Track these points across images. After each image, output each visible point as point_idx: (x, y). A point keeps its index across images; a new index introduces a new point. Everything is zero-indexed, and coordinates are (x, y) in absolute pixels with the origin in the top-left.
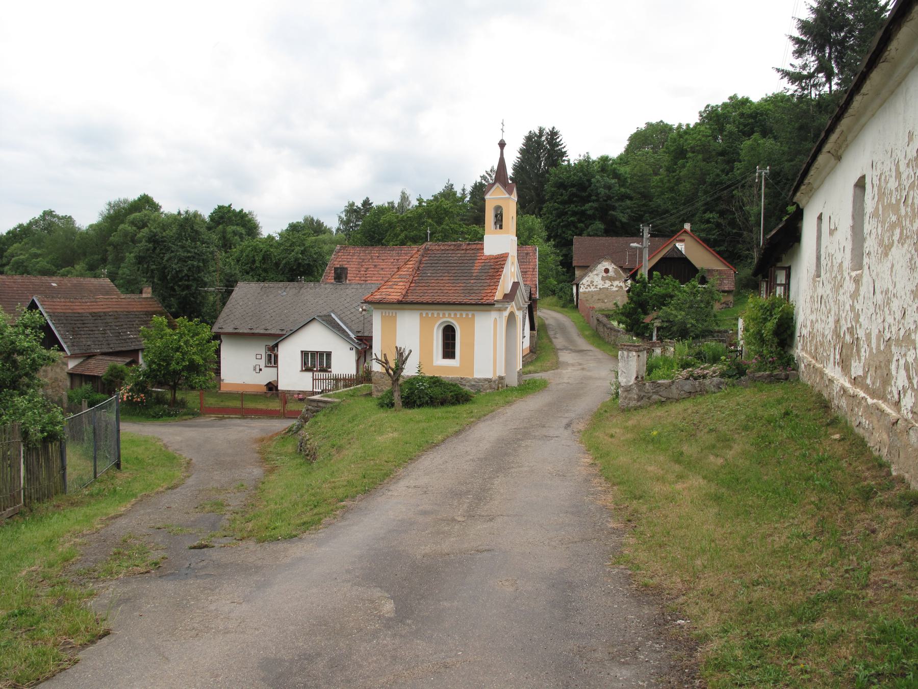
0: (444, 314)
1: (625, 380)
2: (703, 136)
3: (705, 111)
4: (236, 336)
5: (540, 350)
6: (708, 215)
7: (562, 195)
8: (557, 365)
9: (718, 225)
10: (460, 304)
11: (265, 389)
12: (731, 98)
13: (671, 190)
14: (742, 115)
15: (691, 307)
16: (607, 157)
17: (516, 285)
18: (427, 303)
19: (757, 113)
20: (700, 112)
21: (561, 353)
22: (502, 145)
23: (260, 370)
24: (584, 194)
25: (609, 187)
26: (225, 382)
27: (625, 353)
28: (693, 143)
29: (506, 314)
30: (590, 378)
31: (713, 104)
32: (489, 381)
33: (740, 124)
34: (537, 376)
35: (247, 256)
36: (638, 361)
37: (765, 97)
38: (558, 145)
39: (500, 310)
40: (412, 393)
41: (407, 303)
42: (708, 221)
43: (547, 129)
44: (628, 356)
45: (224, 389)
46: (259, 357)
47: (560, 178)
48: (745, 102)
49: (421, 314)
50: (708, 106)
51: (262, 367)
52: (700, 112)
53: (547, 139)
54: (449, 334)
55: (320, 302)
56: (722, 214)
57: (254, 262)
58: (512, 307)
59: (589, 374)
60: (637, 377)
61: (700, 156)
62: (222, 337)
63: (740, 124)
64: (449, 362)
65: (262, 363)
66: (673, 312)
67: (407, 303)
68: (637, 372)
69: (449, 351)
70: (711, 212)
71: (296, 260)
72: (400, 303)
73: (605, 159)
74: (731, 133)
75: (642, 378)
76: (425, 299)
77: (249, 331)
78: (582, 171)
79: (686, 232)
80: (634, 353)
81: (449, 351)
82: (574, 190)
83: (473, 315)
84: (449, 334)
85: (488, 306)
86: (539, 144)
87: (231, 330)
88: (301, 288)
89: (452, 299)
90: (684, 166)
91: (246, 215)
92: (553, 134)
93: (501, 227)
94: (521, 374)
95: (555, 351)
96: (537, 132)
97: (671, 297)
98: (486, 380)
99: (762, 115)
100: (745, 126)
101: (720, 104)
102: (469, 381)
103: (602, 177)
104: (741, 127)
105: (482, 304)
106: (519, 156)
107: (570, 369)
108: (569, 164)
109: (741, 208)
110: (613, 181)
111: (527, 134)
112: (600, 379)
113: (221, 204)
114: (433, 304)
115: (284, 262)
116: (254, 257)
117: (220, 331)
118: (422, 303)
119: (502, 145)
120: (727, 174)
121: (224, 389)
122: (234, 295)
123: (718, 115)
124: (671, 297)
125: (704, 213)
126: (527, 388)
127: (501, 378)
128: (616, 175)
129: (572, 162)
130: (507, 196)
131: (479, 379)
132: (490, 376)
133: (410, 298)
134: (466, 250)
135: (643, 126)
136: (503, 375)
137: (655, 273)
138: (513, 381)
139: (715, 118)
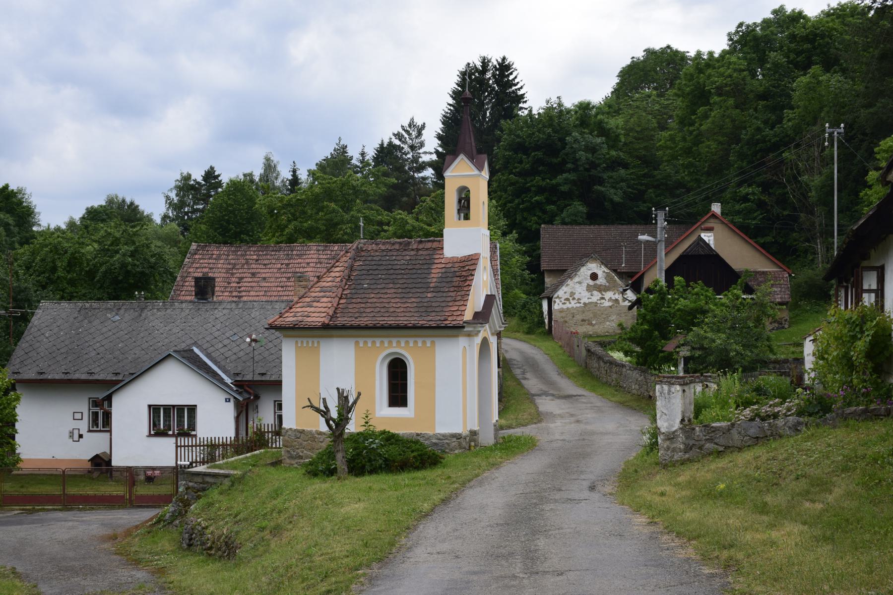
0: (390, 343)
1: (666, 424)
2: (735, 70)
3: (737, 32)
4: (44, 385)
5: (511, 393)
6: (744, 190)
7: (521, 162)
8: (538, 417)
9: (761, 204)
10: (415, 327)
11: (89, 466)
12: (775, 12)
13: (688, 152)
14: (793, 37)
15: (733, 328)
16: (589, 104)
17: (490, 299)
18: (367, 328)
19: (816, 35)
20: (729, 34)
21: (539, 401)
23: (81, 436)
24: (555, 161)
25: (592, 149)
27: (666, 387)
28: (720, 81)
29: (478, 340)
30: (593, 433)
31: (749, 21)
32: (457, 436)
33: (790, 51)
34: (517, 432)
35: (43, 260)
36: (684, 397)
37: (826, 8)
38: (511, 84)
39: (469, 335)
40: (359, 454)
41: (336, 328)
42: (745, 199)
43: (495, 59)
44: (669, 391)
46: (78, 416)
47: (518, 136)
48: (798, 16)
49: (357, 343)
50: (741, 25)
51: (84, 431)
52: (729, 34)
53: (494, 75)
54: (397, 372)
55: (175, 330)
56: (766, 187)
57: (54, 269)
58: (485, 331)
59: (589, 427)
60: (683, 420)
61: (731, 101)
63: (790, 51)
65: (83, 426)
66: (709, 335)
67: (336, 328)
68: (683, 412)
69: (398, 397)
70: (749, 186)
71: (124, 265)
72: (325, 327)
73: (584, 107)
74: (776, 65)
75: (689, 420)
76: (364, 321)
77: (63, 377)
78: (551, 125)
79: (714, 216)
80: (678, 387)
81: (398, 397)
82: (539, 154)
83: (433, 343)
84: (397, 372)
85: (455, 329)
86: (482, 83)
87: (32, 375)
88: (142, 310)
89: (402, 321)
90: (706, 116)
91: (13, 194)
92: (504, 68)
93: (467, 217)
94: (499, 428)
95: (530, 397)
96: (479, 65)
97: (704, 312)
98: (454, 436)
99: (823, 36)
100: (798, 53)
101: (759, 21)
103: (582, 133)
104: (792, 56)
105: (446, 327)
106: (451, 101)
107: (559, 423)
108: (530, 114)
109: (795, 178)
110: (599, 140)
111: (462, 67)
112: (607, 434)
114: (375, 327)
115: (103, 269)
116: (53, 261)
118: (359, 328)
120: (772, 128)
122: (35, 320)
123: (756, 39)
124: (704, 312)
125: (740, 185)
126: (509, 447)
127: (473, 433)
128: (602, 130)
129: (535, 112)
130: (476, 172)
131: (444, 436)
132: (458, 429)
133: (341, 320)
134: (418, 250)
135: (640, 54)
136: (476, 428)
137: (676, 278)
138: (488, 438)
139: (748, 41)
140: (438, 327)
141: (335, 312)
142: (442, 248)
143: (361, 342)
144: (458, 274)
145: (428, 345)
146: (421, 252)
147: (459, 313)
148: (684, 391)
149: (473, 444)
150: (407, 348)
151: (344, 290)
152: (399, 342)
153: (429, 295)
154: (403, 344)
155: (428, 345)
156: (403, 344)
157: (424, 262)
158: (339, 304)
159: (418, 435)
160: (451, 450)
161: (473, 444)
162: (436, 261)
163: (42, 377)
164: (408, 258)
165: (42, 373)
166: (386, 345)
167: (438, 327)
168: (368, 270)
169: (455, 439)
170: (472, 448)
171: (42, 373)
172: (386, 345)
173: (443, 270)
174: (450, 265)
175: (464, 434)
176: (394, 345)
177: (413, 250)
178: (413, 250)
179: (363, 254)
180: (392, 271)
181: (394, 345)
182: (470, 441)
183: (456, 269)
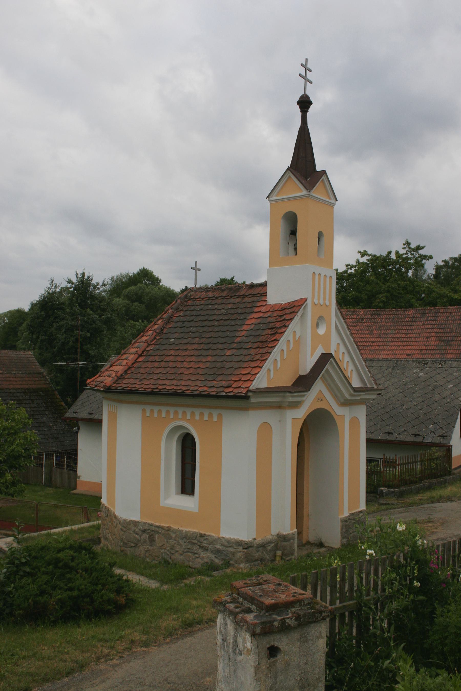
22: (305, 104)
26: (82, 479)
32: (247, 546)
41: (123, 392)
45: (80, 489)
49: (144, 411)
62: (80, 423)
64: (188, 503)
83: (220, 416)
85: (241, 400)
89: (183, 385)
93: (296, 254)
98: (239, 543)
102: (213, 542)
113: (222, 277)
114: (152, 393)
117: (75, 415)
119: (305, 104)
121: (80, 489)
130: (304, 192)
131: (229, 541)
133: (126, 384)
134: (244, 296)
140: (217, 397)
141: (126, 372)
142: (266, 293)
143: (148, 409)
144: (271, 325)
145: (215, 419)
146: (246, 299)
147: (248, 377)
148: (273, 651)
149: (279, 553)
150: (189, 419)
151: (149, 345)
152: (184, 413)
153: (228, 353)
154: (188, 417)
155: (215, 419)
156: (188, 417)
157: (243, 311)
158: (135, 362)
159: (202, 536)
160: (236, 562)
161: (279, 553)
162: (256, 310)
163: (91, 417)
164: (230, 306)
165: (91, 414)
166: (172, 416)
167: (217, 397)
168: (183, 322)
169: (240, 549)
170: (278, 559)
171: (91, 414)
172: (172, 416)
173: (258, 321)
174: (269, 314)
175: (259, 540)
176: (180, 416)
177: (239, 296)
178: (239, 296)
179: (190, 303)
180: (206, 323)
181: (180, 416)
182: (276, 548)
183: (272, 320)
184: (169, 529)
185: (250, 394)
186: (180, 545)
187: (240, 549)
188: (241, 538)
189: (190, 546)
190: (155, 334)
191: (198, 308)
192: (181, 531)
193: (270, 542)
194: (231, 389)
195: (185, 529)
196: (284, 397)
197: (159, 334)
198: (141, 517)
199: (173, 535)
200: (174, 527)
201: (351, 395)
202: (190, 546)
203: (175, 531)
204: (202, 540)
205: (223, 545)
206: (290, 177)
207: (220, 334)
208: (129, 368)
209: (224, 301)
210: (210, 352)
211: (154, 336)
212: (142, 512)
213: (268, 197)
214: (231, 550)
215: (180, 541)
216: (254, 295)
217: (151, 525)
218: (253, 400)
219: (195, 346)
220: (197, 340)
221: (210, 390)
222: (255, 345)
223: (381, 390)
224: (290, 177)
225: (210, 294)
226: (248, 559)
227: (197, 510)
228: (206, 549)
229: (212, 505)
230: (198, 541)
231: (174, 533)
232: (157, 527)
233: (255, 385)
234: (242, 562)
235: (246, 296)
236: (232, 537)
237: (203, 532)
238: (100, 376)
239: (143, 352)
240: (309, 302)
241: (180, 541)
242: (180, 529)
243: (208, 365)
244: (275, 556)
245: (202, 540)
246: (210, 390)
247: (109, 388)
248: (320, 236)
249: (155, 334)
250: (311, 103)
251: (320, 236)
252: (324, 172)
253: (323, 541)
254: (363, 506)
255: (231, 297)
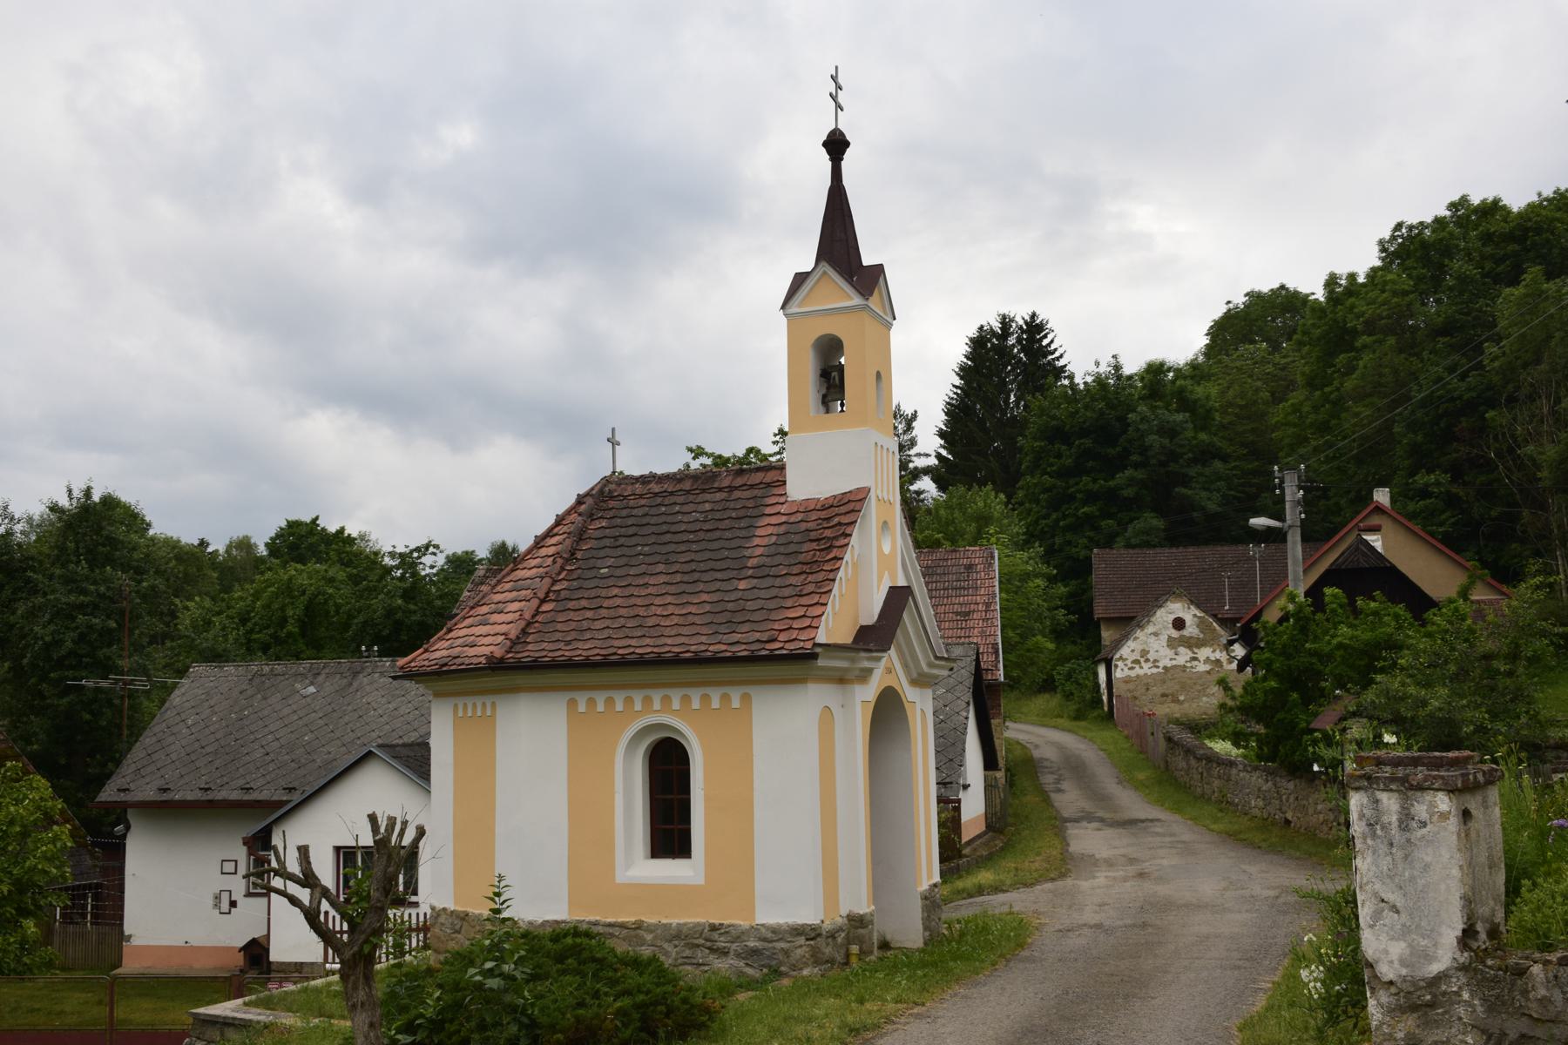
0: (647, 701)
1: (1397, 949)
2: (1395, 293)
3: (1393, 238)
4: (172, 812)
5: (1015, 823)
6: (1421, 479)
7: (1059, 456)
8: (1064, 865)
9: (1451, 501)
10: (698, 661)
11: (240, 959)
12: (1453, 206)
13: (1323, 428)
14: (1487, 238)
15: (1460, 676)
16: (1162, 364)
17: (898, 598)
18: (588, 665)
19: (1527, 230)
20: (1381, 242)
21: (1073, 831)
22: (836, 145)
23: (233, 904)
24: (1112, 451)
25: (1171, 432)
26: (135, 942)
27: (1390, 802)
28: (1369, 311)
29: (868, 693)
30: (1167, 906)
31: (1413, 220)
32: (810, 933)
33: (1483, 257)
34: (998, 903)
35: (267, 606)
36: (1467, 839)
37: (1535, 199)
38: (1045, 351)
39: (841, 679)
40: (458, 1006)
42: (1424, 493)
43: (1020, 314)
44: (1406, 818)
45: (130, 965)
46: (229, 867)
47: (1054, 418)
48: (1492, 209)
49: (572, 703)
50: (1399, 226)
51: (238, 895)
52: (1381, 242)
53: (1019, 340)
54: (668, 768)
55: (404, 709)
56: (1456, 473)
57: (283, 621)
58: (887, 670)
59: (1163, 890)
60: (1468, 934)
61: (1391, 340)
62: (131, 816)
63: (1483, 257)
64: (670, 870)
65: (238, 886)
66: (1412, 690)
68: (1468, 902)
69: (670, 835)
70: (1430, 471)
71: (390, 612)
72: (496, 666)
73: (1155, 370)
74: (1463, 280)
75: (1493, 933)
76: (585, 649)
77: (197, 795)
78: (1104, 398)
79: (1379, 509)
80: (1443, 802)
81: (670, 835)
82: (1088, 442)
83: (746, 699)
84: (668, 768)
85: (794, 663)
86: (1003, 352)
87: (148, 793)
88: (356, 674)
89: (671, 645)
90: (1351, 369)
91: (350, 540)
92: (1035, 328)
94: (931, 903)
95: (1059, 825)
96: (997, 326)
97: (1397, 647)
98: (798, 931)
99: (1538, 230)
100: (1502, 260)
101: (1429, 220)
102: (739, 935)
103: (1153, 408)
104: (1488, 266)
105: (772, 658)
106: (958, 382)
107: (1101, 878)
108: (1073, 386)
109: (1511, 451)
110: (1180, 417)
111: (972, 332)
112: (1199, 906)
113: (292, 518)
114: (605, 664)
115: (361, 618)
116: (283, 609)
117: (122, 797)
118: (569, 665)
119: (836, 145)
120: (1463, 377)
121: (130, 965)
122: (176, 698)
123: (1424, 245)
124: (1397, 647)
125: (1412, 474)
126: (956, 951)
127: (858, 922)
128: (1184, 402)
129: (1078, 380)
130: (856, 300)
131: (775, 930)
132: (808, 913)
133: (534, 649)
134: (731, 489)
135: (1240, 300)
136: (864, 908)
137: (1328, 591)
138: (907, 928)
139: (1413, 251)
140: (753, 659)
141: (524, 632)
142: (784, 483)
143: (582, 700)
144: (813, 535)
145: (736, 704)
146: (737, 494)
147: (807, 622)
148: (1466, 815)
149: (855, 949)
150: (681, 712)
151: (554, 582)
152: (666, 700)
153: (742, 585)
154: (676, 705)
155: (736, 704)
156: (676, 705)
157: (742, 513)
158: (537, 612)
159: (713, 928)
160: (794, 967)
161: (855, 949)
162: (768, 510)
163: (165, 797)
164: (707, 506)
165: (165, 790)
166: (638, 707)
167: (753, 659)
168: (616, 538)
169: (802, 940)
170: (854, 960)
171: (165, 790)
172: (638, 707)
173: (782, 529)
174: (800, 517)
175: (827, 926)
176: (657, 705)
177: (720, 489)
178: (720, 489)
179: (612, 504)
180: (668, 537)
181: (657, 705)
182: (849, 941)
183: (811, 525)
184: (639, 925)
185: (818, 650)
186: (666, 954)
187: (802, 940)
188: (800, 922)
189: (688, 953)
190: (560, 561)
191: (639, 512)
192: (667, 927)
193: (841, 929)
194: (777, 645)
195: (675, 921)
196: (853, 660)
197: (567, 560)
198: (570, 912)
199: (649, 937)
200: (650, 920)
201: (930, 665)
202: (688, 953)
203: (651, 929)
204: (715, 935)
205: (764, 940)
206: (825, 273)
207: (707, 555)
208: (529, 624)
209: (691, 498)
210: (701, 586)
211: (558, 565)
212: (570, 903)
213: (783, 307)
214: (782, 945)
215: (666, 946)
216: (752, 486)
217: (596, 924)
218: (821, 662)
219: (662, 579)
220: (661, 567)
221: (734, 649)
222: (796, 570)
223: (954, 660)
224: (825, 273)
225: (656, 488)
226: (817, 959)
227: (701, 880)
228: (724, 953)
229: (738, 864)
230: (711, 939)
231: (652, 932)
232: (610, 925)
233: (822, 638)
234: (806, 965)
235: (736, 488)
236: (781, 921)
237: (717, 922)
238: (426, 651)
239: (547, 594)
240: (872, 494)
241: (666, 946)
242: (664, 921)
243: (707, 608)
244: (848, 955)
245: (715, 935)
246: (734, 649)
247: (502, 660)
248: (878, 375)
249: (560, 561)
250: (847, 144)
251: (878, 375)
252: (879, 269)
253: (888, 937)
254: (937, 879)
255: (704, 491)
